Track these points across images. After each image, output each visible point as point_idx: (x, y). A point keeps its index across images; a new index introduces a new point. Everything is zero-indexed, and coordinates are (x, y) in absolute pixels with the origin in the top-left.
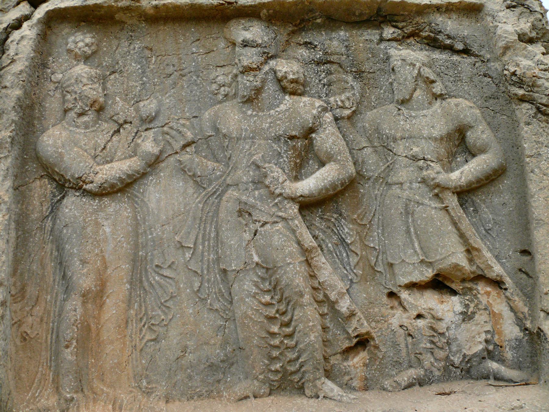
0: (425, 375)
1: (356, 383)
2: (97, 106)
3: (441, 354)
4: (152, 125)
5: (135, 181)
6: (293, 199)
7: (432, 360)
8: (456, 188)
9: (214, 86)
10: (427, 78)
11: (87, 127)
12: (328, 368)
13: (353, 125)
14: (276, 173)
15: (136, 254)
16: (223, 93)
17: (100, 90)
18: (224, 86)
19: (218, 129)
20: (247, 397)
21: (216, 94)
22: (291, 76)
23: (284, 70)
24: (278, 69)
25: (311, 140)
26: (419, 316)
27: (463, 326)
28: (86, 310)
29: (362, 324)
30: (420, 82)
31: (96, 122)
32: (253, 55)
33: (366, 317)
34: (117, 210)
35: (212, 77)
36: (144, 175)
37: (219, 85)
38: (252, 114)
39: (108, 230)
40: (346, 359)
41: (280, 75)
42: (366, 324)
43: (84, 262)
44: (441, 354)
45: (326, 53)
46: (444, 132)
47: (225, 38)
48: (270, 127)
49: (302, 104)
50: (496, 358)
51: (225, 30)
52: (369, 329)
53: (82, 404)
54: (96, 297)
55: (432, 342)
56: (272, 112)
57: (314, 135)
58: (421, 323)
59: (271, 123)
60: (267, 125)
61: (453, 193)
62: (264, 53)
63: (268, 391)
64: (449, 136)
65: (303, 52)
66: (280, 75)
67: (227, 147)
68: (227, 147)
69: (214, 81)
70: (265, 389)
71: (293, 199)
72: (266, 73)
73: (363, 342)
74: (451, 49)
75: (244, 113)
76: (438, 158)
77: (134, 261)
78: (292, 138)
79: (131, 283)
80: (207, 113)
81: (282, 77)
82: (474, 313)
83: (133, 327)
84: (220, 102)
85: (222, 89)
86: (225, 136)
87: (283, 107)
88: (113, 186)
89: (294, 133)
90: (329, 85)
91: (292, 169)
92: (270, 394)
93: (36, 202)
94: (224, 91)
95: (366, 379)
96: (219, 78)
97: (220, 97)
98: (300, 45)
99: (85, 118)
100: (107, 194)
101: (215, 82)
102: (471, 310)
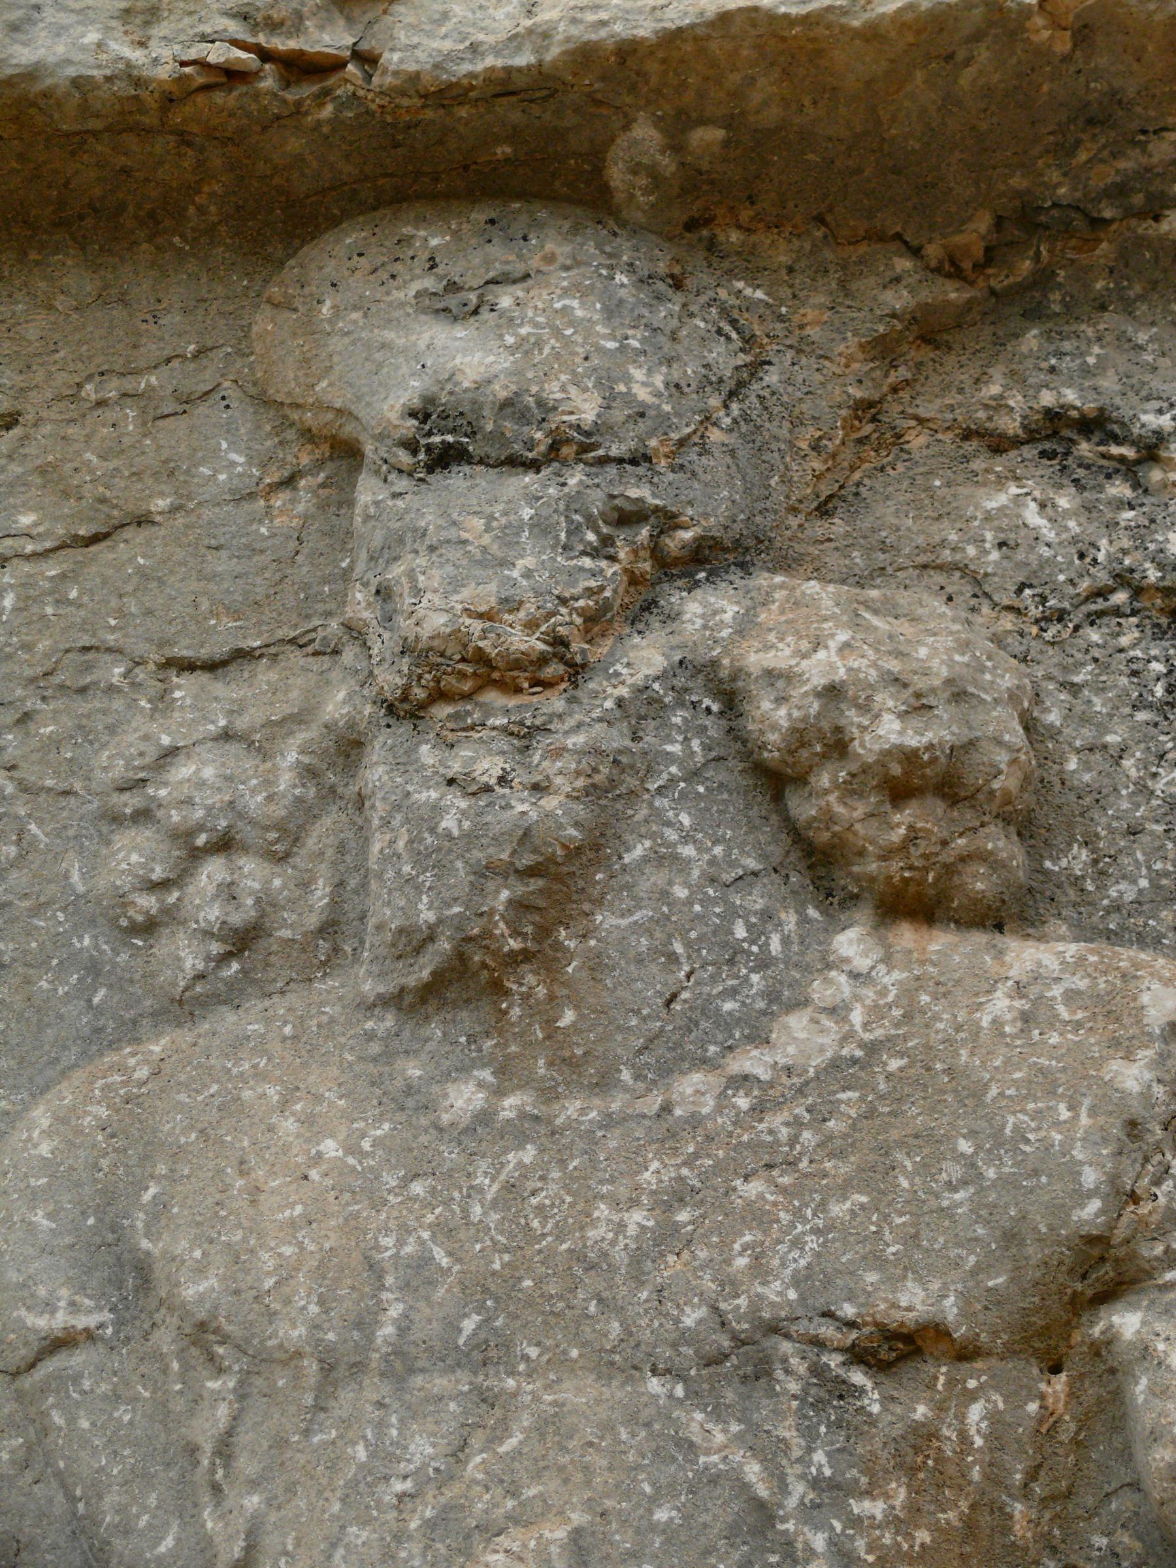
9: (134, 854)
16: (213, 914)
18: (224, 845)
19: (143, 1270)
21: (149, 927)
22: (888, 731)
23: (819, 668)
24: (755, 660)
25: (1107, 1366)
32: (509, 535)
35: (112, 762)
37: (183, 836)
38: (484, 1117)
41: (773, 718)
47: (263, 401)
48: (666, 1237)
49: (1001, 1004)
51: (264, 322)
56: (692, 1088)
57: (1127, 1322)
59: (680, 1195)
60: (637, 1218)
62: (627, 517)
65: (1032, 513)
66: (773, 718)
67: (225, 1449)
68: (225, 1449)
69: (130, 802)
72: (642, 709)
75: (414, 1102)
78: (896, 1349)
80: (41, 1116)
81: (799, 736)
84: (184, 1007)
85: (213, 871)
86: (202, 1334)
87: (802, 1039)
89: (913, 1301)
94: (229, 892)
96: (183, 771)
97: (184, 955)
98: (999, 445)
101: (143, 816)
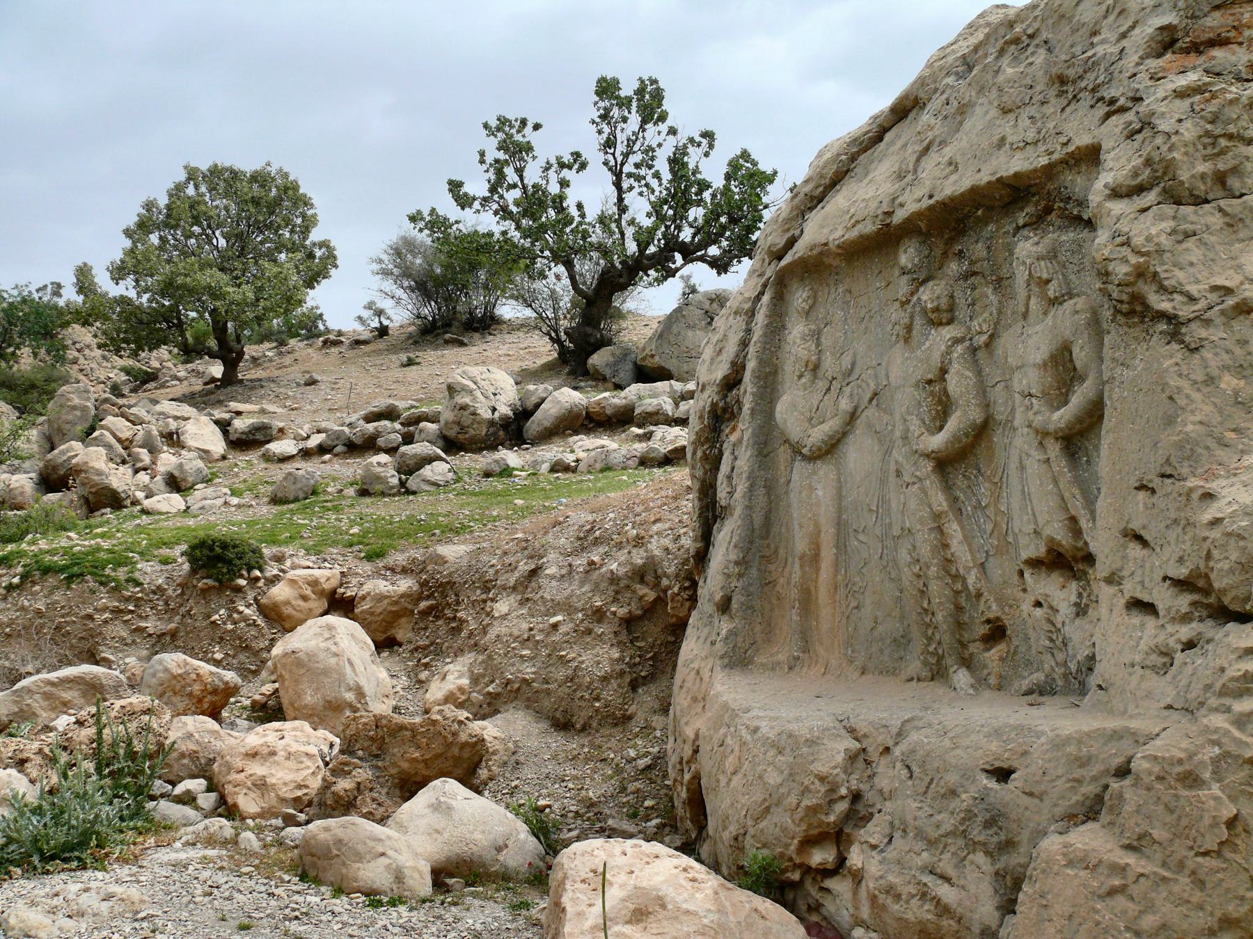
0: (1046, 682)
1: (993, 680)
2: (811, 366)
3: (1060, 657)
4: (851, 379)
5: (839, 441)
6: (927, 456)
7: (1053, 663)
8: (1056, 432)
10: (1040, 278)
11: (805, 389)
12: (967, 656)
13: (991, 354)
14: (915, 427)
15: (839, 517)
17: (813, 347)
20: (912, 679)
26: (1038, 604)
27: (1078, 621)
28: (804, 573)
29: (990, 607)
30: (1033, 287)
31: (813, 382)
33: (996, 600)
34: (825, 471)
36: (845, 434)
39: (820, 493)
40: (989, 650)
42: (994, 607)
43: (801, 527)
44: (1060, 657)
45: (972, 263)
46: (1046, 356)
50: (289, 711)
52: (999, 614)
53: (806, 665)
54: (813, 559)
55: (1052, 640)
58: (1039, 612)
61: (1057, 439)
62: (914, 280)
63: (929, 675)
64: (1053, 357)
70: (925, 673)
71: (927, 456)
74: (296, 500)
76: (1043, 392)
77: (838, 524)
78: (930, 382)
79: (837, 547)
82: (1087, 606)
83: (842, 592)
88: (819, 449)
89: (930, 376)
90: (974, 304)
91: (934, 419)
92: (932, 679)
93: (783, 468)
95: (1001, 676)
99: (803, 380)
100: (819, 457)
102: (1084, 601)
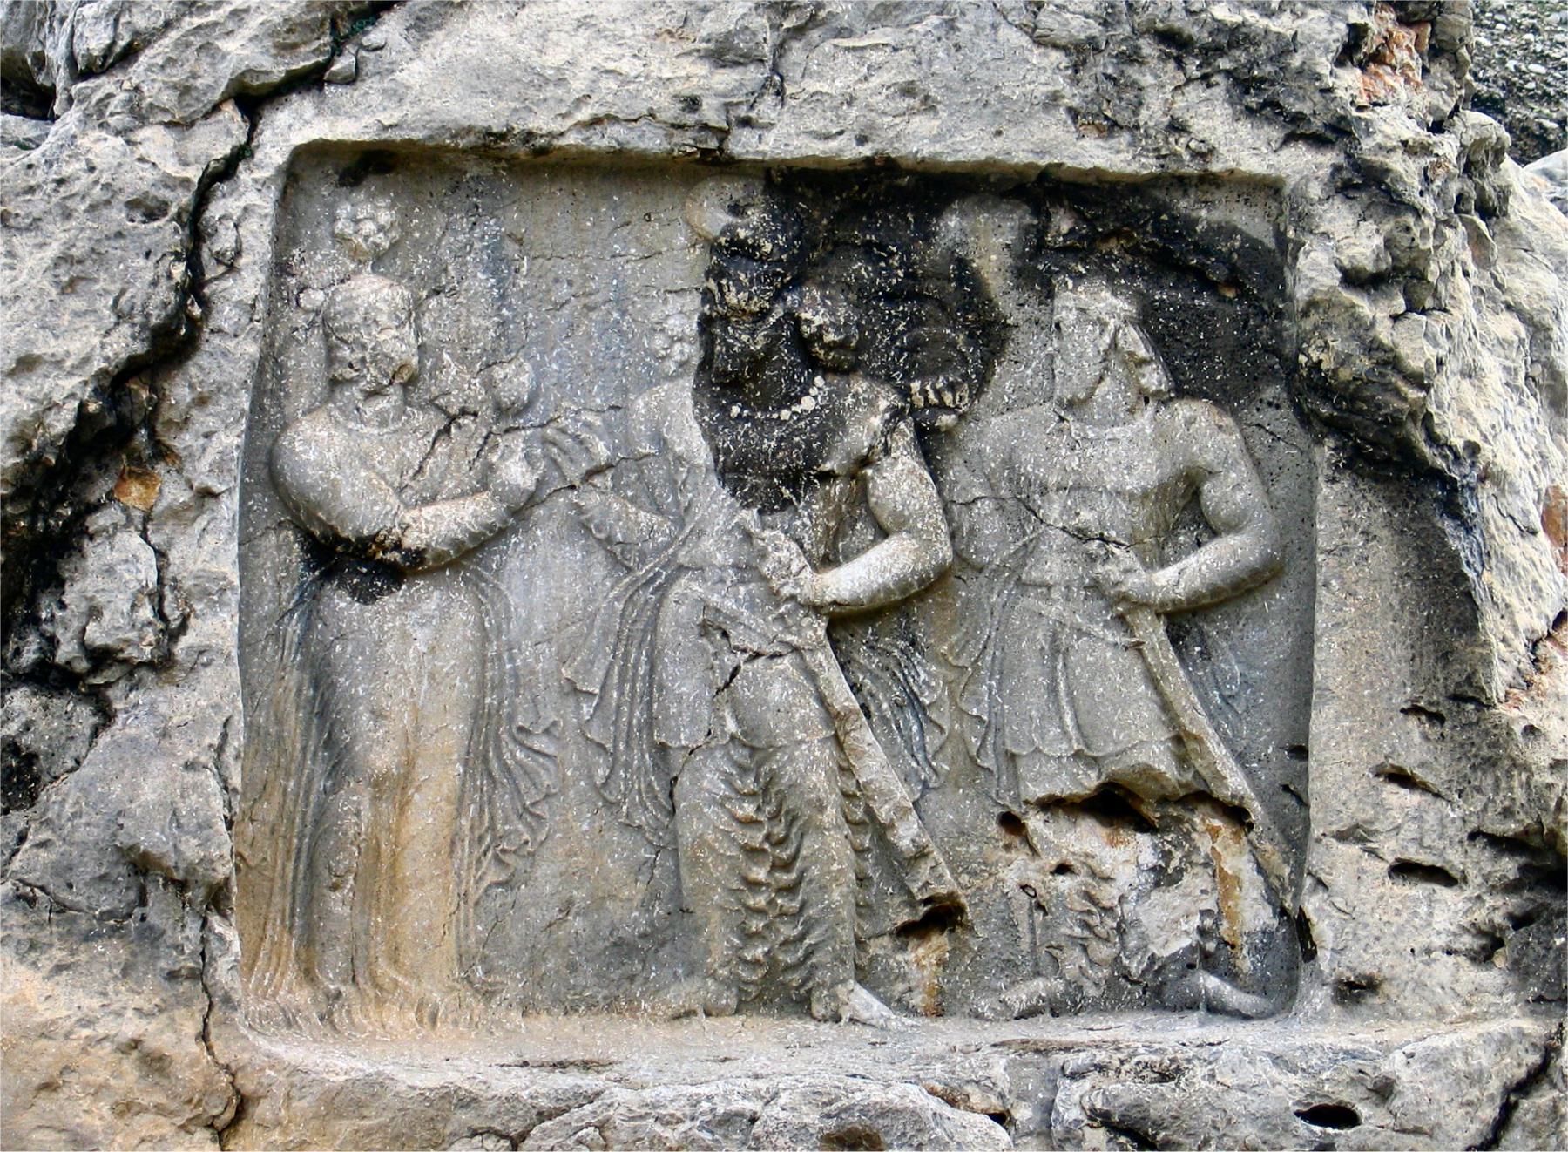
0: (1066, 993)
3: (1104, 952)
7: (1084, 962)
9: (659, 342)
12: (865, 962)
15: (479, 702)
18: (680, 340)
19: (665, 441)
20: (689, 1013)
21: (663, 358)
22: (830, 337)
23: (818, 320)
24: (804, 315)
25: (863, 483)
26: (1063, 869)
27: (1155, 896)
29: (941, 876)
32: (751, 281)
33: (948, 862)
35: (654, 316)
37: (672, 337)
38: (740, 415)
40: (903, 948)
41: (806, 330)
42: (948, 876)
44: (1104, 952)
47: (688, 223)
49: (850, 400)
51: (689, 204)
55: (1086, 925)
56: (785, 414)
57: (869, 472)
58: (1064, 883)
59: (780, 440)
60: (773, 444)
63: (733, 1003)
66: (806, 330)
67: (684, 483)
68: (684, 483)
69: (659, 328)
70: (729, 999)
71: (816, 609)
72: (778, 324)
73: (942, 916)
79: (466, 764)
80: (640, 401)
81: (812, 335)
82: (1180, 871)
84: (670, 378)
85: (677, 347)
86: (679, 459)
87: (808, 403)
91: (820, 541)
92: (737, 1012)
94: (682, 352)
95: (941, 992)
96: (671, 321)
97: (672, 367)
99: (382, 404)
101: (662, 330)
102: (1174, 863)
